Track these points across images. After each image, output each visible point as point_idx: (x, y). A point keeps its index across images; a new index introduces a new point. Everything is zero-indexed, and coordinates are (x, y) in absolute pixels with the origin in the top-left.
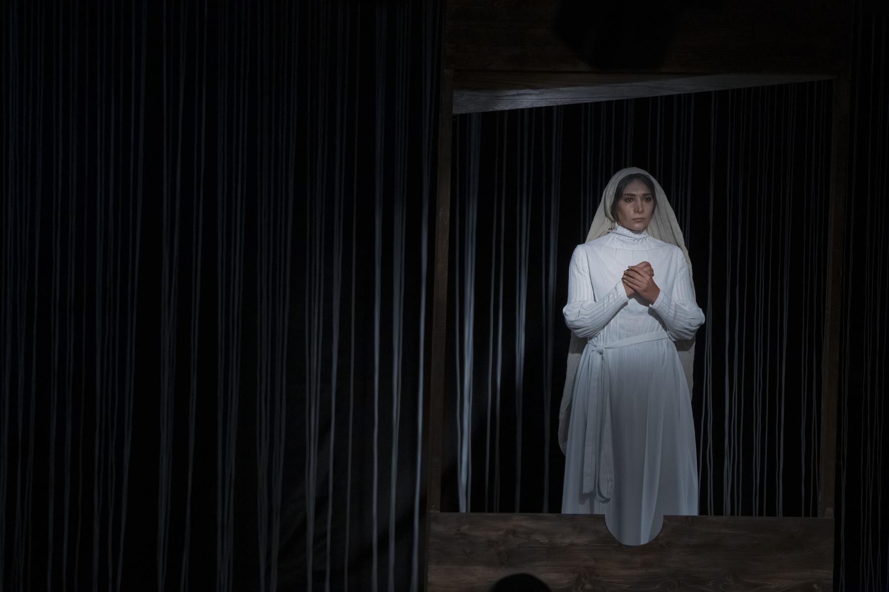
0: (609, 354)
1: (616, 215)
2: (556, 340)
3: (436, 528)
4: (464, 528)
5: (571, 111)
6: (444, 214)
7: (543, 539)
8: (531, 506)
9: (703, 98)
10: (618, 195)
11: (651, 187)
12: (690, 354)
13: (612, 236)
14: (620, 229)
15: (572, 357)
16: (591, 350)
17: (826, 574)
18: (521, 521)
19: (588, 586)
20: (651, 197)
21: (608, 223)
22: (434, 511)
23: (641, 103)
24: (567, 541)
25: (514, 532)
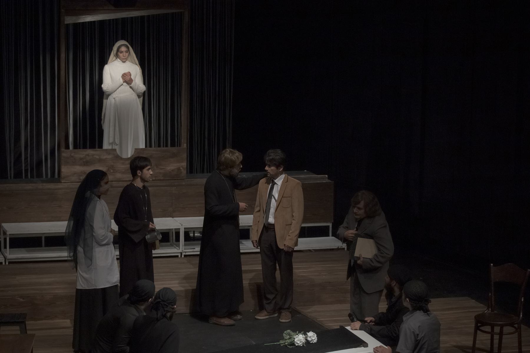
0: (117, 99)
1: (117, 56)
2: (99, 95)
3: (64, 155)
4: (72, 154)
5: (102, 23)
6: (63, 56)
7: (97, 157)
8: (92, 147)
9: (142, 17)
10: (118, 50)
11: (128, 48)
12: (142, 98)
13: (116, 62)
14: (119, 60)
15: (105, 101)
16: (111, 98)
17: (184, 164)
18: (90, 152)
19: (112, 171)
20: (128, 51)
21: (115, 58)
22: (63, 149)
23: (124, 20)
24: (105, 157)
25: (88, 155)
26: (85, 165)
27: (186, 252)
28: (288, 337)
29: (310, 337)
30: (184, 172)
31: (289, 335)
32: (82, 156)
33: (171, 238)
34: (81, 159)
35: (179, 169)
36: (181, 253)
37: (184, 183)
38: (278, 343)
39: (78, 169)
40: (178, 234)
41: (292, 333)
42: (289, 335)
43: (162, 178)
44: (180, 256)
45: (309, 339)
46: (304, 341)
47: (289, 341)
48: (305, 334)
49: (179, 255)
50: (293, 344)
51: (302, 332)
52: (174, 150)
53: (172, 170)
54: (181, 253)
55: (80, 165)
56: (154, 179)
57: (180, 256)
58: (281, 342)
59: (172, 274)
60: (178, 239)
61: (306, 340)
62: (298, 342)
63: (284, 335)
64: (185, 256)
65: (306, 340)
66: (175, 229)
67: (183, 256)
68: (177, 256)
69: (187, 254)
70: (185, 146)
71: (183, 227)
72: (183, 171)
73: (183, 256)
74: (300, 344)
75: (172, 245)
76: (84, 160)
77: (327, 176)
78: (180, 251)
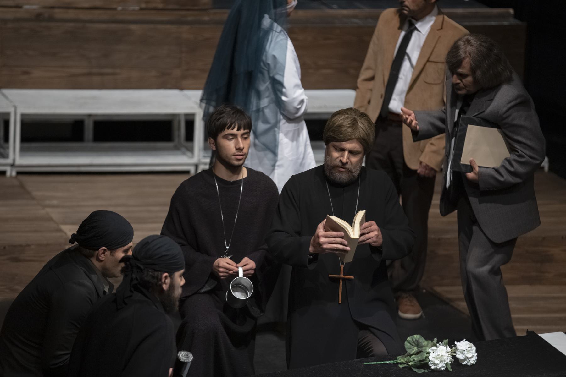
28: (415, 349)
29: (462, 352)
31: (418, 344)
33: (176, 133)
36: (197, 166)
37: (206, 18)
38: (393, 362)
40: (190, 124)
41: (424, 343)
42: (418, 344)
43: (160, 6)
45: (460, 356)
46: (449, 359)
47: (416, 358)
48: (451, 344)
50: (424, 364)
51: (446, 341)
54: (197, 166)
56: (143, 6)
58: (400, 359)
60: (190, 137)
61: (454, 357)
62: (437, 362)
63: (407, 345)
65: (454, 357)
66: (186, 115)
68: (187, 172)
74: (441, 366)
75: (177, 148)
77: (511, 11)
78: (195, 160)
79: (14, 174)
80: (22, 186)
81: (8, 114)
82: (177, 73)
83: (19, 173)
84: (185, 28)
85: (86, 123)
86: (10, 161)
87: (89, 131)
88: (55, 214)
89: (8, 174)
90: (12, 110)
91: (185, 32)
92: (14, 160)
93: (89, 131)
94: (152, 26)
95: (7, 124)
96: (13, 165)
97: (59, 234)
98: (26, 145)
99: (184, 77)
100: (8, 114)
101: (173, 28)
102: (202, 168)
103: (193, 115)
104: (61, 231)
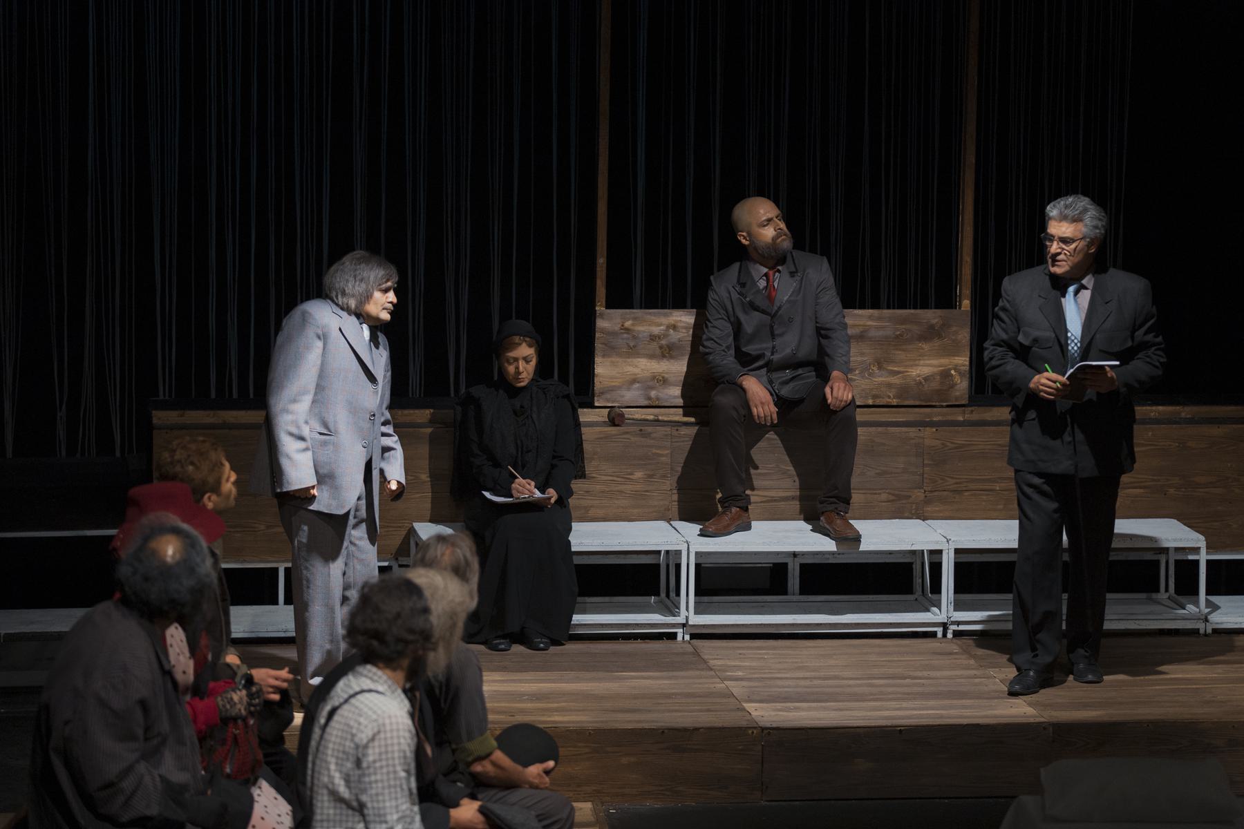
3: (601, 324)
4: (628, 324)
17: (963, 361)
22: (600, 308)
25: (674, 327)
26: (663, 356)
27: (958, 623)
30: (962, 386)
32: (656, 330)
34: (653, 338)
35: (945, 375)
39: (644, 366)
40: (936, 568)
44: (940, 635)
49: (940, 631)
52: (932, 316)
53: (926, 379)
54: (945, 626)
55: (651, 357)
56: (870, 402)
57: (940, 635)
59: (908, 681)
64: (957, 634)
66: (932, 552)
67: (950, 635)
68: (934, 635)
69: (962, 628)
70: (966, 303)
71: (953, 546)
72: (957, 379)
73: (950, 635)
76: (663, 342)
78: (941, 618)
79: (687, 637)
80: (696, 653)
81: (679, 553)
82: (919, 495)
83: (693, 636)
84: (929, 431)
85: (790, 567)
86: (680, 620)
87: (794, 581)
88: (736, 688)
89: (680, 638)
90: (684, 548)
91: (928, 436)
92: (687, 618)
93: (794, 581)
94: (880, 429)
95: (678, 566)
96: (684, 625)
97: (740, 713)
98: (706, 599)
99: (928, 501)
100: (679, 553)
101: (912, 432)
102: (954, 627)
103: (940, 552)
104: (744, 709)
